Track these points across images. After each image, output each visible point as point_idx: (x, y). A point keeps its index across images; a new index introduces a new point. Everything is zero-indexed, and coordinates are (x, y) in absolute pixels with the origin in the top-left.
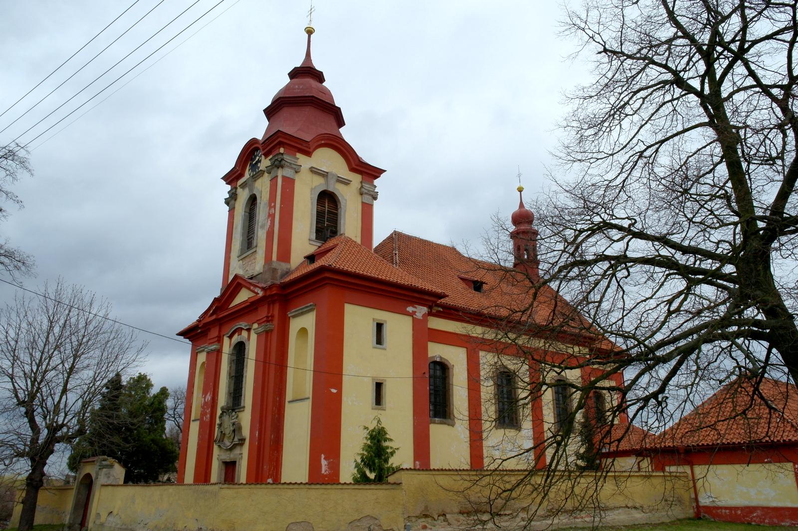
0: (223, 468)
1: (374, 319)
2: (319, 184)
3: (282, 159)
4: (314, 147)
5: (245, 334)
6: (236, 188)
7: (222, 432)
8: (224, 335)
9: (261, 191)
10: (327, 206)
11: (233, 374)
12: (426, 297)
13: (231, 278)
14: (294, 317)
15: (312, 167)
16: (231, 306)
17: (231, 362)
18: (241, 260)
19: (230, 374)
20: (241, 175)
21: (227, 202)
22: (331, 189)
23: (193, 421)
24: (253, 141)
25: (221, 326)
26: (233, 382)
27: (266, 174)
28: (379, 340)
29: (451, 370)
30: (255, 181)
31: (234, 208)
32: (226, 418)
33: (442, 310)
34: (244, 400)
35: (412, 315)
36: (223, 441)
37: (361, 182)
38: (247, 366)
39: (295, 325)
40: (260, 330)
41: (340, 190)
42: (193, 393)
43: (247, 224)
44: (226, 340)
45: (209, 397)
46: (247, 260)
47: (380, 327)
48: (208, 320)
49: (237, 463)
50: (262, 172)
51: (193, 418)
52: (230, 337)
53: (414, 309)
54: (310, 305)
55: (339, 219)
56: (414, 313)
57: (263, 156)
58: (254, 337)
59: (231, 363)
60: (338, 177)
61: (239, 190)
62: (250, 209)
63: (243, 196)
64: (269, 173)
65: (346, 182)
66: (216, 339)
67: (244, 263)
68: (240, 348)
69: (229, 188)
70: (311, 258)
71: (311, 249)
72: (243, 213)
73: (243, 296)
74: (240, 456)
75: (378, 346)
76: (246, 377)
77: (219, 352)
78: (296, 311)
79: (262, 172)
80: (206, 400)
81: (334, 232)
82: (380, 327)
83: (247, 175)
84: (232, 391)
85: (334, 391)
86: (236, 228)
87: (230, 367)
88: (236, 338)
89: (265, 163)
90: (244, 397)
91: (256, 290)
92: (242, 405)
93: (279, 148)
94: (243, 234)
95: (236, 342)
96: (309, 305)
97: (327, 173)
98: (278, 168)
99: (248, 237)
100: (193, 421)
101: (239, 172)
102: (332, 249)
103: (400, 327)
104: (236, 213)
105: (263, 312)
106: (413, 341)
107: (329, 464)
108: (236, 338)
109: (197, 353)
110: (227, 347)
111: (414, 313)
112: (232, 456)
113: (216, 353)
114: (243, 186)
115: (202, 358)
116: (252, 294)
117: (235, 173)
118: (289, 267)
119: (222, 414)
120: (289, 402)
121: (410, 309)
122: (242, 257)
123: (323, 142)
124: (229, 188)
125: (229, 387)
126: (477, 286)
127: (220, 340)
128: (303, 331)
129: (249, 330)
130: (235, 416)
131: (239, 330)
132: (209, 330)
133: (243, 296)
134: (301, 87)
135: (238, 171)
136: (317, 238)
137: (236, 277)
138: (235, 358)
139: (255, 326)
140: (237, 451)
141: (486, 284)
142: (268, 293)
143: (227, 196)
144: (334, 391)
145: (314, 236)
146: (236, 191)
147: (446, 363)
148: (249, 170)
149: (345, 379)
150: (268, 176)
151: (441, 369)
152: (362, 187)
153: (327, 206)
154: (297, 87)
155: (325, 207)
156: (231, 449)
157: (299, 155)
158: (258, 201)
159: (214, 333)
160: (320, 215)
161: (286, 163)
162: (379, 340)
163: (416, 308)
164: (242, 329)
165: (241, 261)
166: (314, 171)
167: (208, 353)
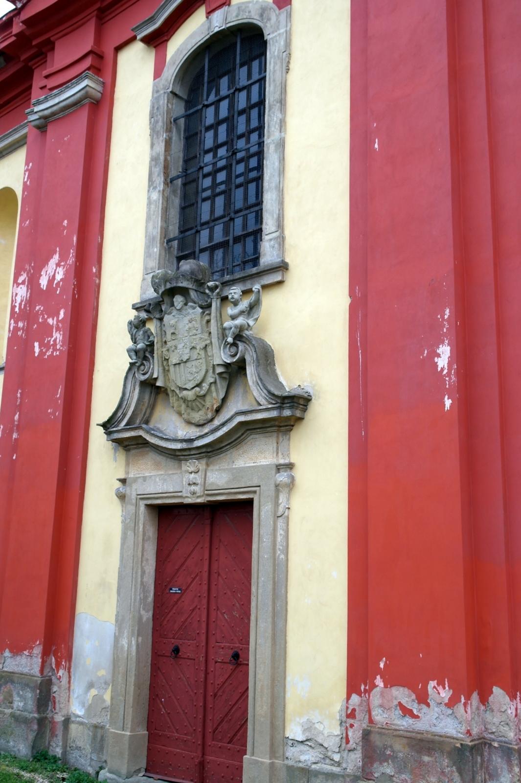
19: (166, 168)
32: (184, 323)
36: (147, 422)
38: (282, 103)
45: (55, 271)
49: (262, 513)
52: (157, 40)
66: (88, 62)
74: (282, 477)
76: (281, 145)
80: (44, 282)
84: (174, 231)
90: (280, 226)
92: (268, 255)
110: (139, 83)
113: (83, 117)
119: (151, 310)
125: (165, 218)
127: (101, 64)
130: (244, 304)
140: (255, 459)
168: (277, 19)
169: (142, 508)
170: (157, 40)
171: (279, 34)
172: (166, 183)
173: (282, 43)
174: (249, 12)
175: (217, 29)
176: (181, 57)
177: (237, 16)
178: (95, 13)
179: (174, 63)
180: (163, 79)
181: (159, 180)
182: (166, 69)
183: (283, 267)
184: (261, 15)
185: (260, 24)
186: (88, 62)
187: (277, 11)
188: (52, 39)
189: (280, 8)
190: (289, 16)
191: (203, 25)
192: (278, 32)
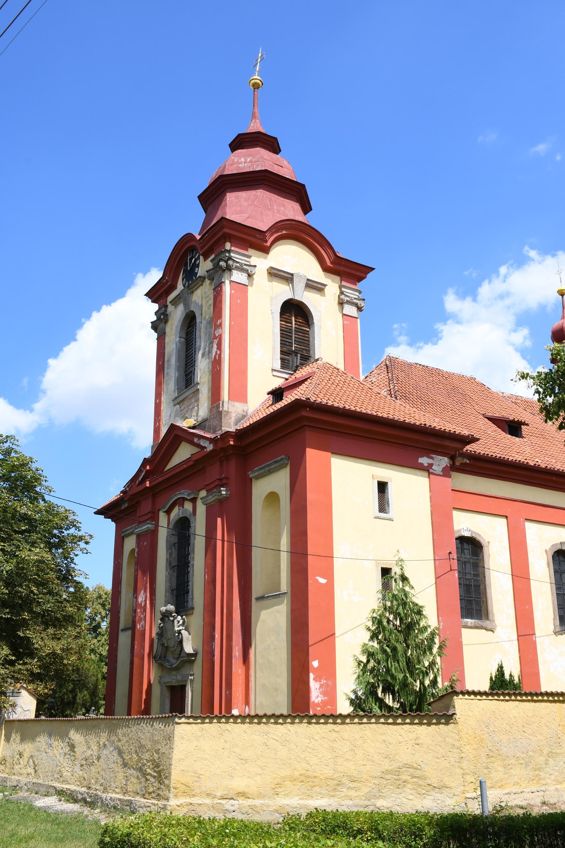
0: (167, 694)
1: (373, 476)
2: (284, 292)
3: (230, 258)
4: (272, 238)
5: (188, 506)
6: (166, 306)
7: (163, 645)
8: (159, 510)
10: (294, 323)
11: (175, 563)
12: (447, 443)
13: (164, 431)
14: (258, 478)
15: (272, 268)
16: (167, 469)
17: (170, 546)
18: (178, 404)
20: (173, 287)
21: (155, 326)
22: (298, 298)
23: (122, 630)
24: (188, 237)
26: (175, 574)
27: (207, 282)
28: (383, 506)
29: (485, 550)
30: (193, 292)
31: (165, 333)
33: (468, 462)
34: (192, 599)
35: (427, 470)
36: (165, 657)
37: (340, 287)
39: (261, 489)
40: (211, 499)
41: (309, 299)
42: (120, 592)
43: (183, 354)
44: (163, 519)
46: (186, 403)
47: (382, 487)
48: (136, 490)
50: (203, 279)
51: (122, 626)
52: (168, 512)
53: (430, 461)
54: (282, 459)
55: (311, 339)
56: (431, 465)
57: (201, 258)
58: (201, 509)
59: (171, 548)
60: (308, 280)
61: (170, 308)
62: (187, 333)
63: (177, 315)
64: (212, 279)
65: (318, 288)
66: (150, 515)
67: (182, 408)
68: (183, 527)
69: (156, 307)
70: (277, 394)
71: (277, 383)
72: (178, 339)
73: (184, 453)
75: (382, 515)
77: (154, 533)
78: (260, 469)
79: (203, 279)
81: (306, 357)
82: (382, 487)
83: (180, 286)
84: (174, 586)
85: (322, 581)
86: (169, 361)
87: (171, 554)
88: (176, 513)
89: (204, 266)
90: (192, 594)
91: (203, 443)
92: (190, 605)
93: (225, 243)
94: (178, 368)
96: (279, 458)
97: (292, 275)
98: (224, 270)
100: (122, 630)
101: (169, 283)
102: (306, 380)
103: (411, 488)
104: (167, 340)
105: (213, 473)
106: (431, 506)
107: (321, 686)
108: (176, 513)
109: (123, 537)
111: (431, 465)
112: (179, 677)
114: (175, 302)
115: (130, 543)
116: (195, 450)
117: (164, 285)
118: (246, 409)
120: (258, 599)
121: (424, 461)
122: (178, 401)
123: (284, 232)
124: (156, 307)
126: (514, 428)
128: (273, 497)
129: (194, 501)
131: (180, 502)
132: (139, 503)
133: (184, 453)
134: (249, 160)
135: (167, 281)
136: (282, 367)
137: (173, 427)
138: (175, 539)
139: (203, 493)
141: (527, 425)
142: (220, 445)
143: (154, 318)
144: (322, 581)
145: (278, 365)
146: (166, 311)
147: (478, 538)
148: (183, 279)
149: (337, 563)
150: (211, 284)
151: (471, 547)
152: (342, 293)
153: (294, 323)
154: (243, 160)
155: (291, 323)
156: (177, 669)
157: (251, 252)
158: (198, 320)
159: (146, 507)
160: (285, 334)
161: (235, 264)
162: (383, 506)
163: (432, 458)
164: (184, 499)
166: (275, 274)
167: (139, 536)
169: (164, 687)
172: (170, 569)
181: (168, 568)
183: (193, 608)
186: (150, 515)
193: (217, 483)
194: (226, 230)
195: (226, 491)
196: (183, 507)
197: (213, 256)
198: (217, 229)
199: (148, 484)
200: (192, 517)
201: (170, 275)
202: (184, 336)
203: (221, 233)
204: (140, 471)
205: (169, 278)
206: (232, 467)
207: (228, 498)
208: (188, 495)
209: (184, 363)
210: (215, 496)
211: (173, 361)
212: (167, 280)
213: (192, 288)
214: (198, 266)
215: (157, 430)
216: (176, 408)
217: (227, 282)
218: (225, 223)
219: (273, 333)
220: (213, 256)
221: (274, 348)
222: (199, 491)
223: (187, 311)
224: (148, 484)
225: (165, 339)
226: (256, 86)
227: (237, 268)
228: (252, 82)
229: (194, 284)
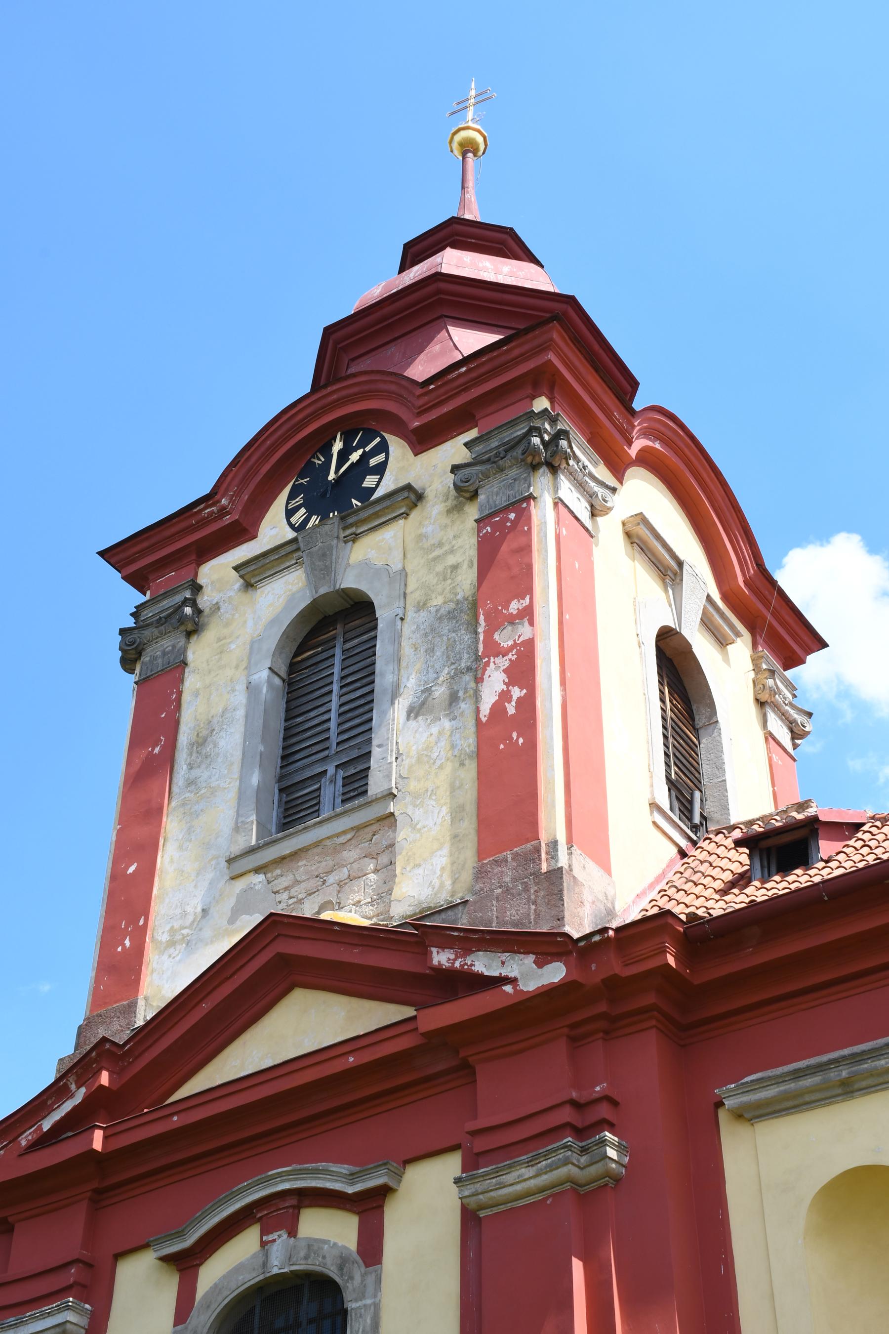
9: (403, 573)
14: (750, 1115)
15: (642, 519)
20: (242, 532)
25: (100, 1199)
31: (185, 663)
43: (278, 724)
46: (303, 867)
73: (305, 1026)
78: (797, 1075)
95: (251, 1278)
98: (535, 467)
99: (281, 778)
101: (227, 520)
123: (657, 445)
129: (370, 1206)
158: (383, 615)
165: (261, 877)
168: (362, 1281)
170: (186, 1263)
171: (365, 1305)
173: (369, 1321)
174: (324, 1257)
175: (275, 1271)
176: (220, 1299)
177: (306, 1258)
178: (89, 1194)
179: (208, 1307)
180: (190, 1327)
182: (194, 1313)
184: (341, 1268)
185: (337, 1279)
187: (363, 1268)
188: (10, 1219)
189: (367, 1266)
190: (378, 1281)
191: (254, 1256)
192: (364, 1302)
193: (566, 1115)
194: (551, 356)
195: (620, 1148)
196: (293, 1233)
197: (473, 434)
198: (516, 352)
199: (98, 1141)
200: (358, 1271)
201: (238, 494)
202: (283, 674)
203: (531, 365)
204: (55, 1092)
205: (231, 501)
206: (640, 1066)
207: (618, 1180)
208: (352, 1178)
209: (280, 752)
210: (566, 1162)
211: (231, 742)
212: (224, 508)
213: (356, 524)
214: (380, 470)
215: (119, 968)
216: (240, 885)
217: (547, 500)
218: (555, 336)
219: (647, 700)
220: (473, 434)
221: (650, 743)
222: (407, 1162)
223: (323, 590)
224: (98, 1141)
225: (181, 680)
226: (468, 148)
227: (572, 475)
228: (463, 134)
229: (370, 511)
